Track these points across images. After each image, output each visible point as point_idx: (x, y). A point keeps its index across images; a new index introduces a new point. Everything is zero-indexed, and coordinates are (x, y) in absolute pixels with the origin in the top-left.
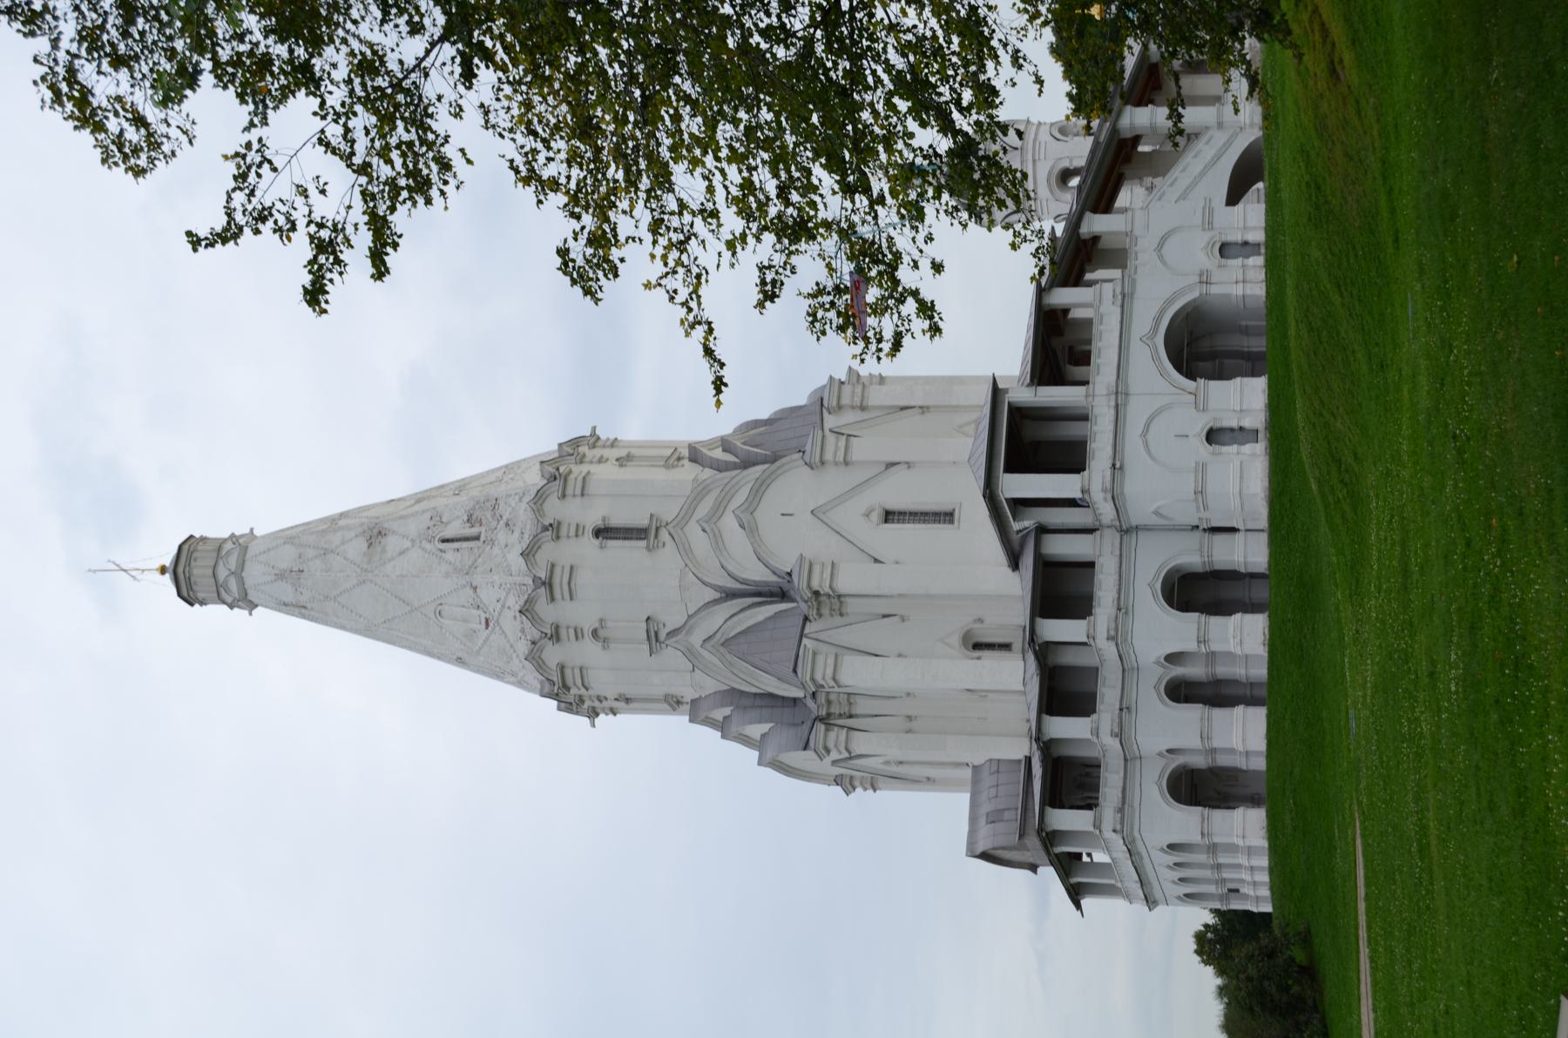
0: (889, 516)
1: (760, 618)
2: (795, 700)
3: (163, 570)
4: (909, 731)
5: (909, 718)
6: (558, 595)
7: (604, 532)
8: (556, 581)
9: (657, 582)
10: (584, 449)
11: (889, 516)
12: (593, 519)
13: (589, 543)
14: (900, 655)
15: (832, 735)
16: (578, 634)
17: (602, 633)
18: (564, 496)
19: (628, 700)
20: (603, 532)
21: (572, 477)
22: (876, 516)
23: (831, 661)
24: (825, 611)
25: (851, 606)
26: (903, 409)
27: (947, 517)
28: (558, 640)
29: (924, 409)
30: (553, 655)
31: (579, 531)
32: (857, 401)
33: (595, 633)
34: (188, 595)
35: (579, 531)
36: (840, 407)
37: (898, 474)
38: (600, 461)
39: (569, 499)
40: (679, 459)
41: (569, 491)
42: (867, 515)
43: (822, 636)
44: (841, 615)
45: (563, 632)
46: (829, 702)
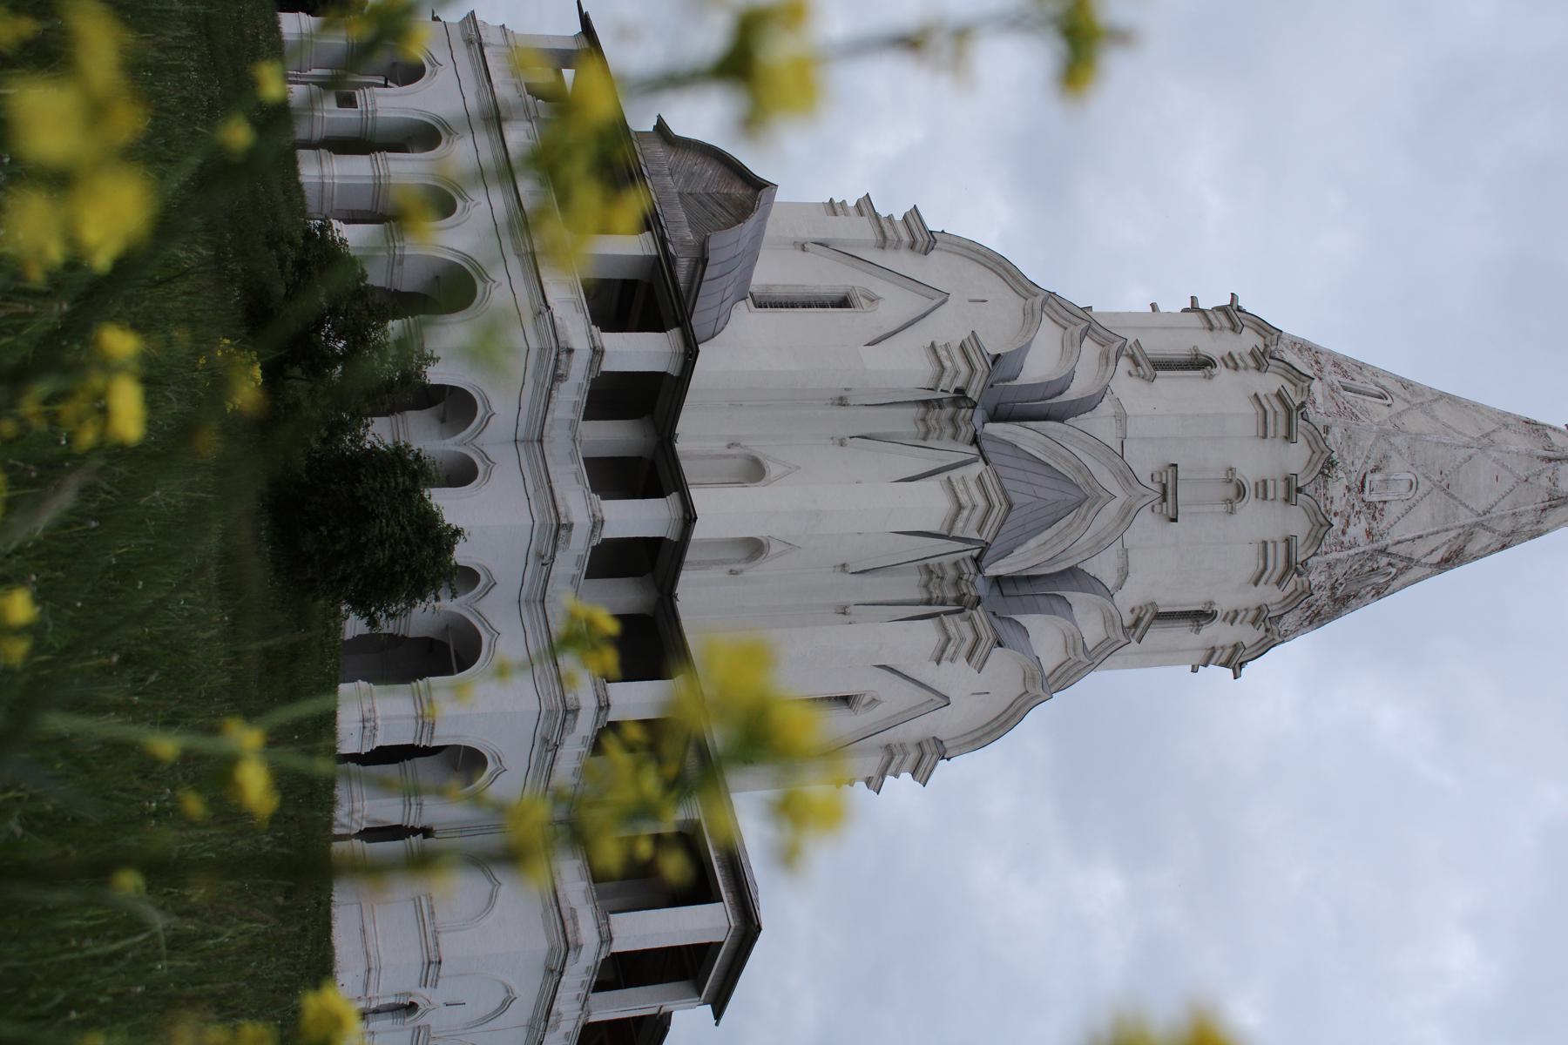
0: (846, 700)
1: (1032, 543)
2: (995, 417)
5: (842, 402)
6: (1281, 547)
7: (1200, 617)
9: (1157, 564)
13: (1223, 605)
15: (959, 383)
16: (1262, 490)
17: (1231, 491)
19: (1200, 364)
20: (1200, 617)
23: (960, 524)
24: (951, 574)
25: (909, 587)
28: (1288, 480)
31: (1233, 617)
33: (1241, 491)
35: (1233, 617)
43: (960, 546)
44: (930, 571)
45: (1281, 494)
46: (953, 420)
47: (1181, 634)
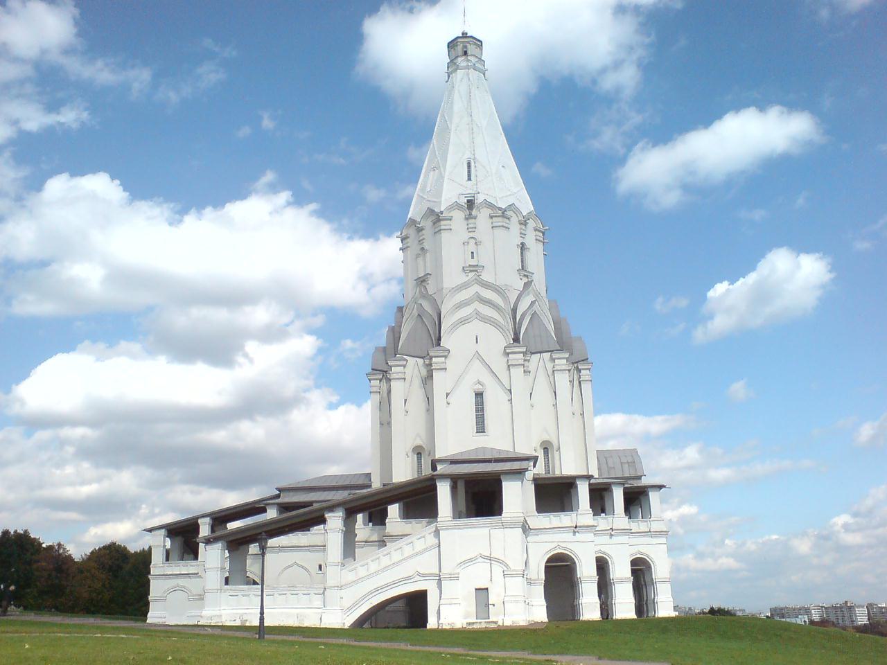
0: (479, 395)
3: (463, 34)
4: (381, 424)
8: (442, 223)
10: (531, 224)
11: (479, 395)
18: (491, 217)
22: (479, 387)
26: (555, 393)
27: (481, 428)
29: (555, 405)
32: (557, 368)
33: (423, 249)
34: (452, 45)
36: (553, 360)
37: (504, 397)
38: (523, 235)
39: (491, 220)
40: (527, 276)
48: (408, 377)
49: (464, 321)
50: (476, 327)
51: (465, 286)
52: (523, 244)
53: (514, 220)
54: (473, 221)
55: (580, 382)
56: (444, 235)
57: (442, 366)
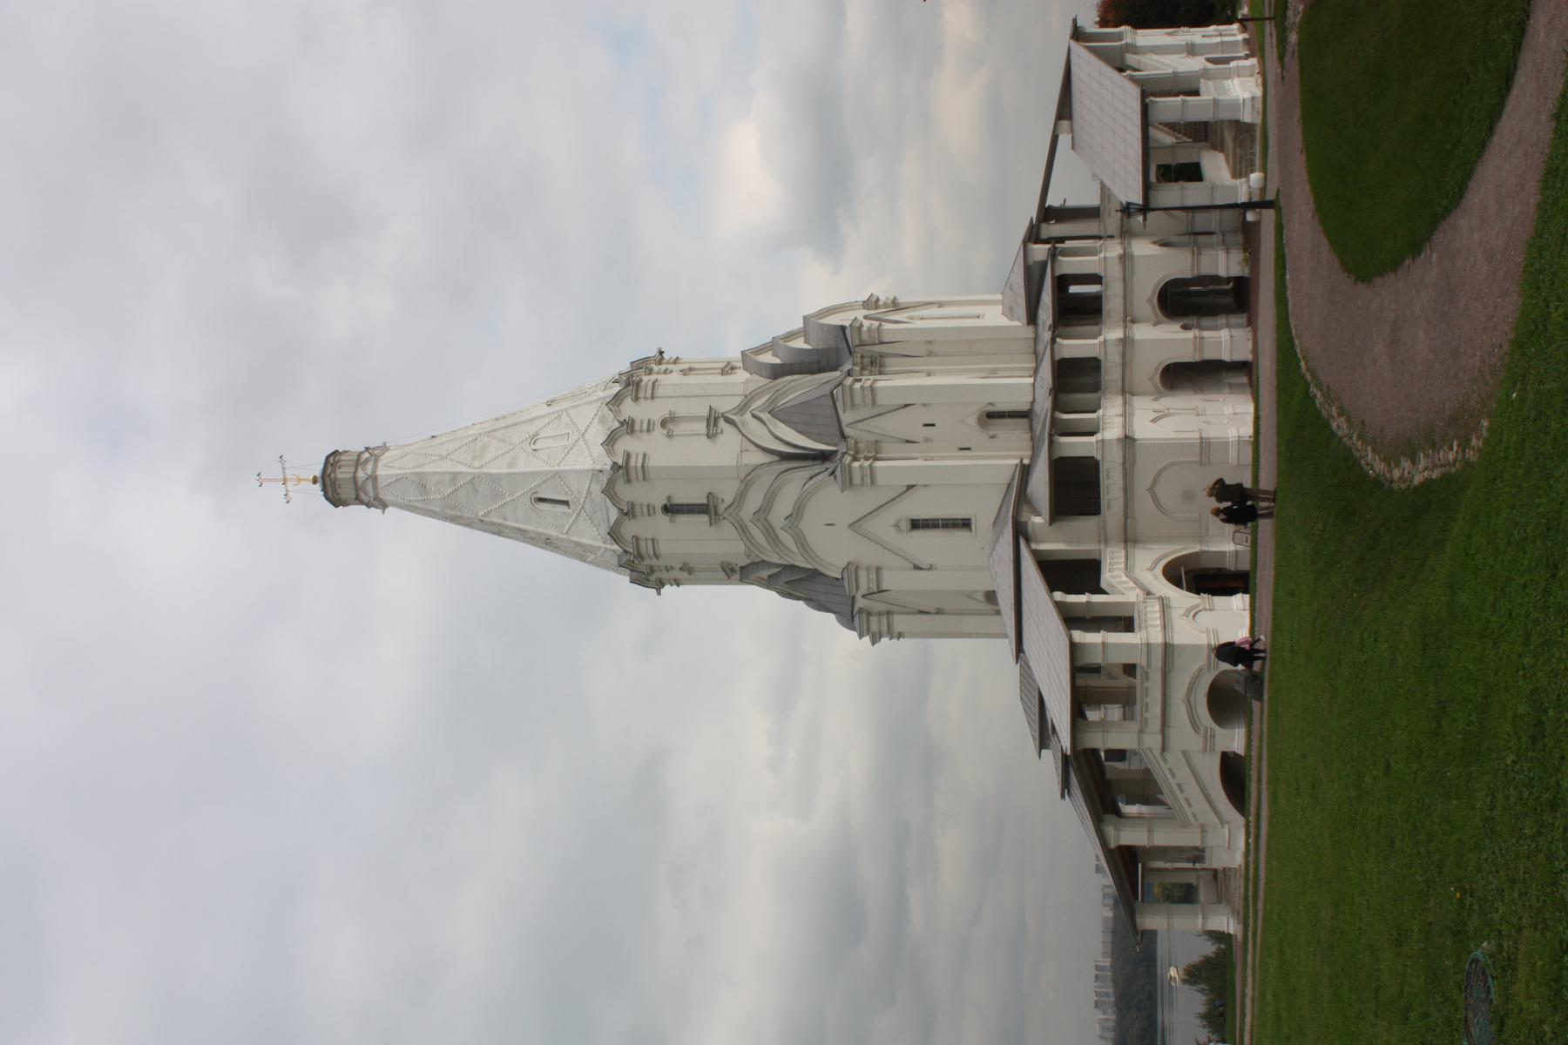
0: (916, 524)
3: (315, 481)
7: (671, 509)
8: (643, 550)
11: (916, 524)
12: (659, 502)
13: (664, 519)
14: (939, 612)
20: (671, 509)
21: (632, 464)
22: (905, 525)
27: (965, 524)
30: (653, 578)
41: (633, 476)
42: (897, 526)
47: (680, 498)
48: (886, 607)
49: (801, 540)
50: (812, 526)
51: (743, 529)
52: (664, 424)
53: (626, 444)
54: (637, 509)
55: (881, 343)
56: (663, 548)
57: (873, 576)
